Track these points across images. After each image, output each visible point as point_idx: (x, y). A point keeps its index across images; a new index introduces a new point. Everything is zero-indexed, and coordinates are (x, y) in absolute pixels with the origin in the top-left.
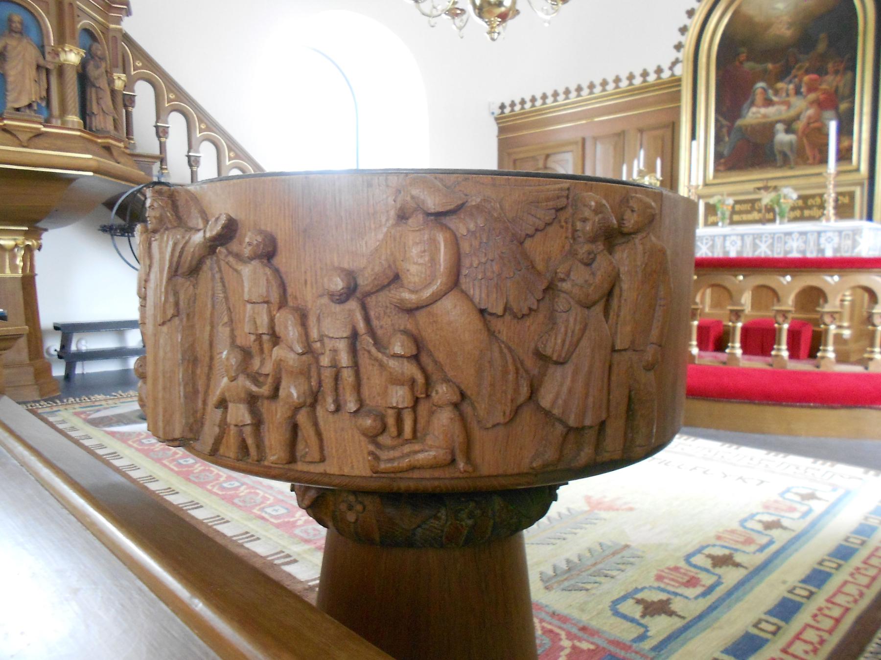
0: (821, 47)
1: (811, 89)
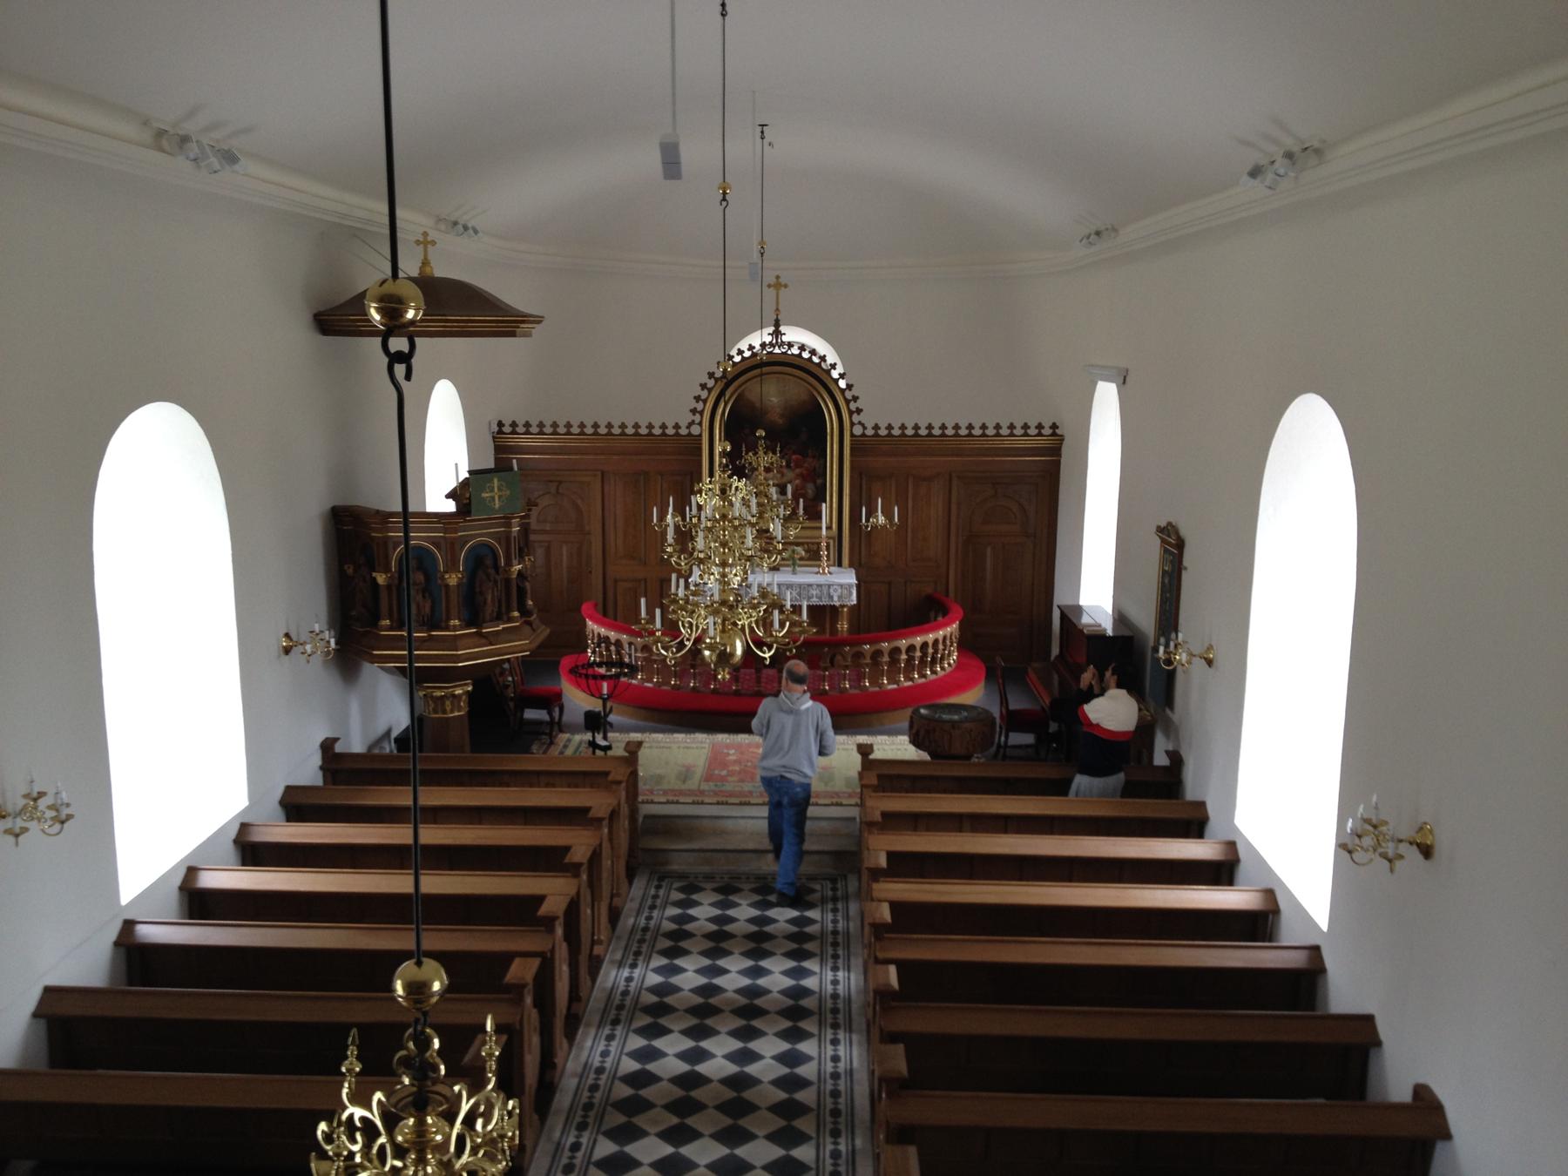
1: (797, 466)
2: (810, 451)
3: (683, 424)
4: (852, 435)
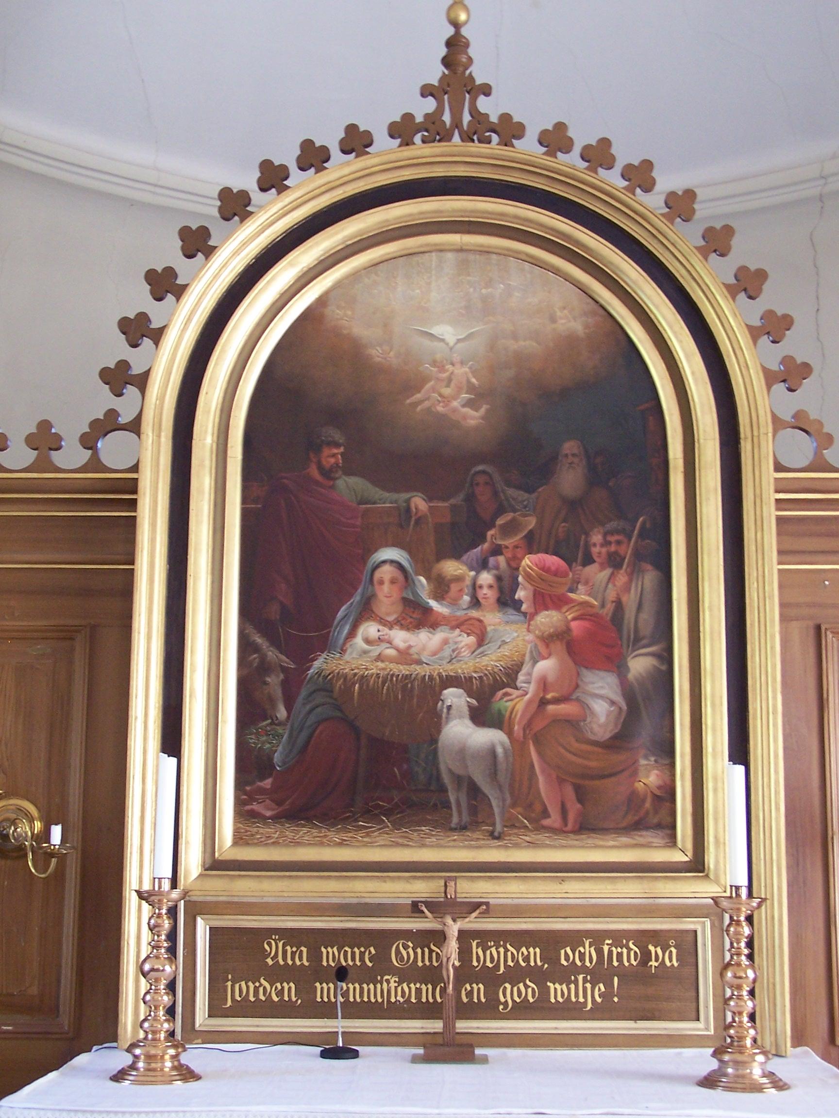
2: (597, 538)
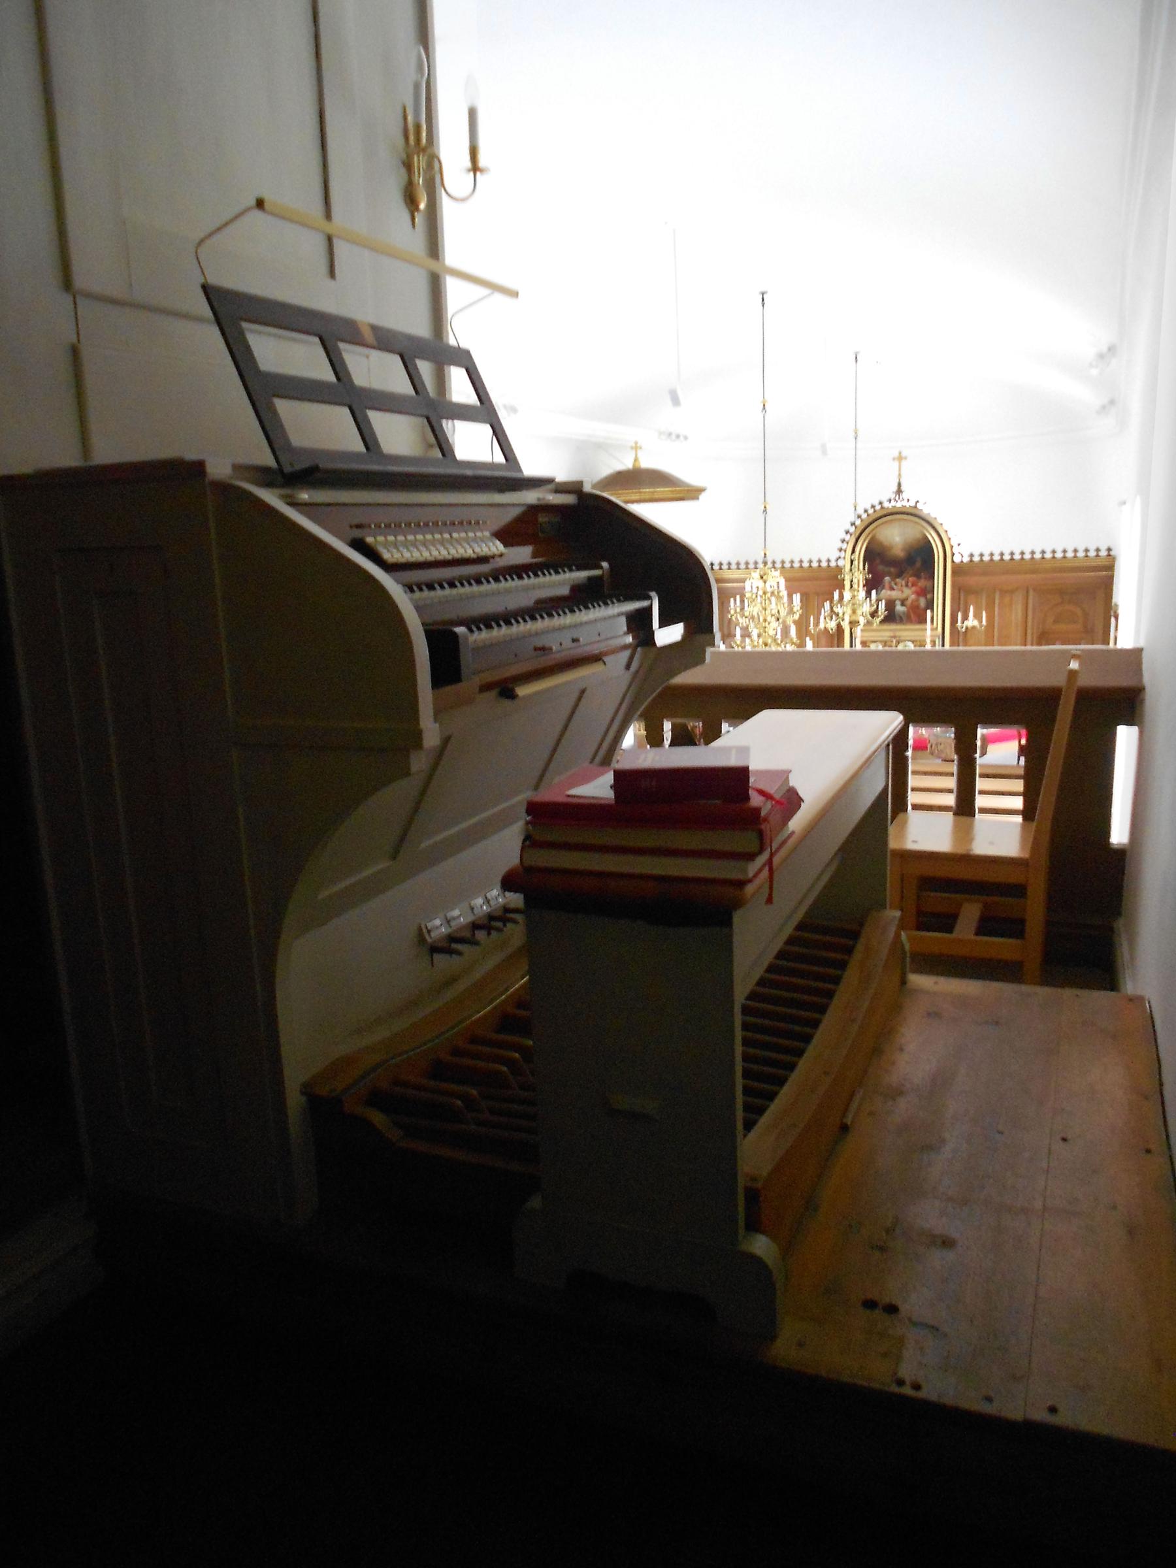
0: (918, 564)
1: (913, 586)
3: (833, 559)
4: (953, 561)
